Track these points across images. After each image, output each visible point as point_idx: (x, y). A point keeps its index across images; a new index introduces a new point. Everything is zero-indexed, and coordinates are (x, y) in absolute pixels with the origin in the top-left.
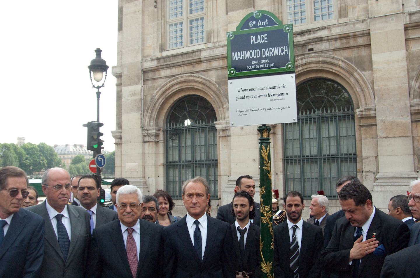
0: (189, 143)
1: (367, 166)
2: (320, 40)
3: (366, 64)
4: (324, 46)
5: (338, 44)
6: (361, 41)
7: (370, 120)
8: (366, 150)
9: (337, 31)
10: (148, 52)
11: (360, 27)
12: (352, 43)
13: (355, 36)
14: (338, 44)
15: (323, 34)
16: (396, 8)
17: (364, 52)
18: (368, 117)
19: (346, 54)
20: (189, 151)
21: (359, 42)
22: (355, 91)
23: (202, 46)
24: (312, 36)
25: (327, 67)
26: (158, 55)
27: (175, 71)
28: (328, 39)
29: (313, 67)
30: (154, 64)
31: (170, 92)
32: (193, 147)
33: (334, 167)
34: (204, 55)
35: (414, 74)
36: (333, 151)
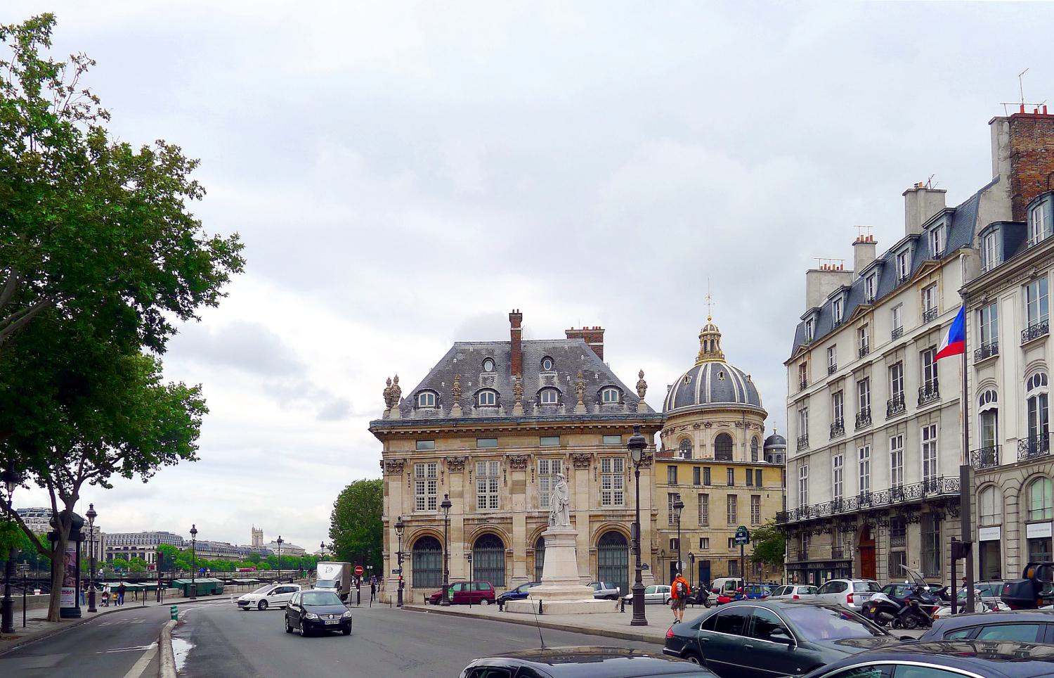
0: (425, 559)
1: (509, 573)
2: (492, 518)
3: (511, 531)
4: (493, 521)
5: (500, 521)
6: (509, 521)
7: (510, 553)
8: (509, 566)
9: (499, 516)
10: (404, 511)
11: (509, 515)
12: (505, 521)
13: (506, 518)
14: (500, 521)
15: (494, 516)
16: (523, 509)
17: (510, 526)
18: (510, 553)
19: (503, 525)
20: (425, 564)
21: (508, 521)
22: (505, 542)
23: (437, 513)
24: (489, 516)
25: (495, 530)
26: (412, 514)
27: (420, 524)
28: (496, 518)
29: (489, 529)
30: (409, 519)
31: (418, 534)
32: (428, 563)
33: (495, 573)
34: (437, 518)
35: (528, 536)
36: (495, 566)
